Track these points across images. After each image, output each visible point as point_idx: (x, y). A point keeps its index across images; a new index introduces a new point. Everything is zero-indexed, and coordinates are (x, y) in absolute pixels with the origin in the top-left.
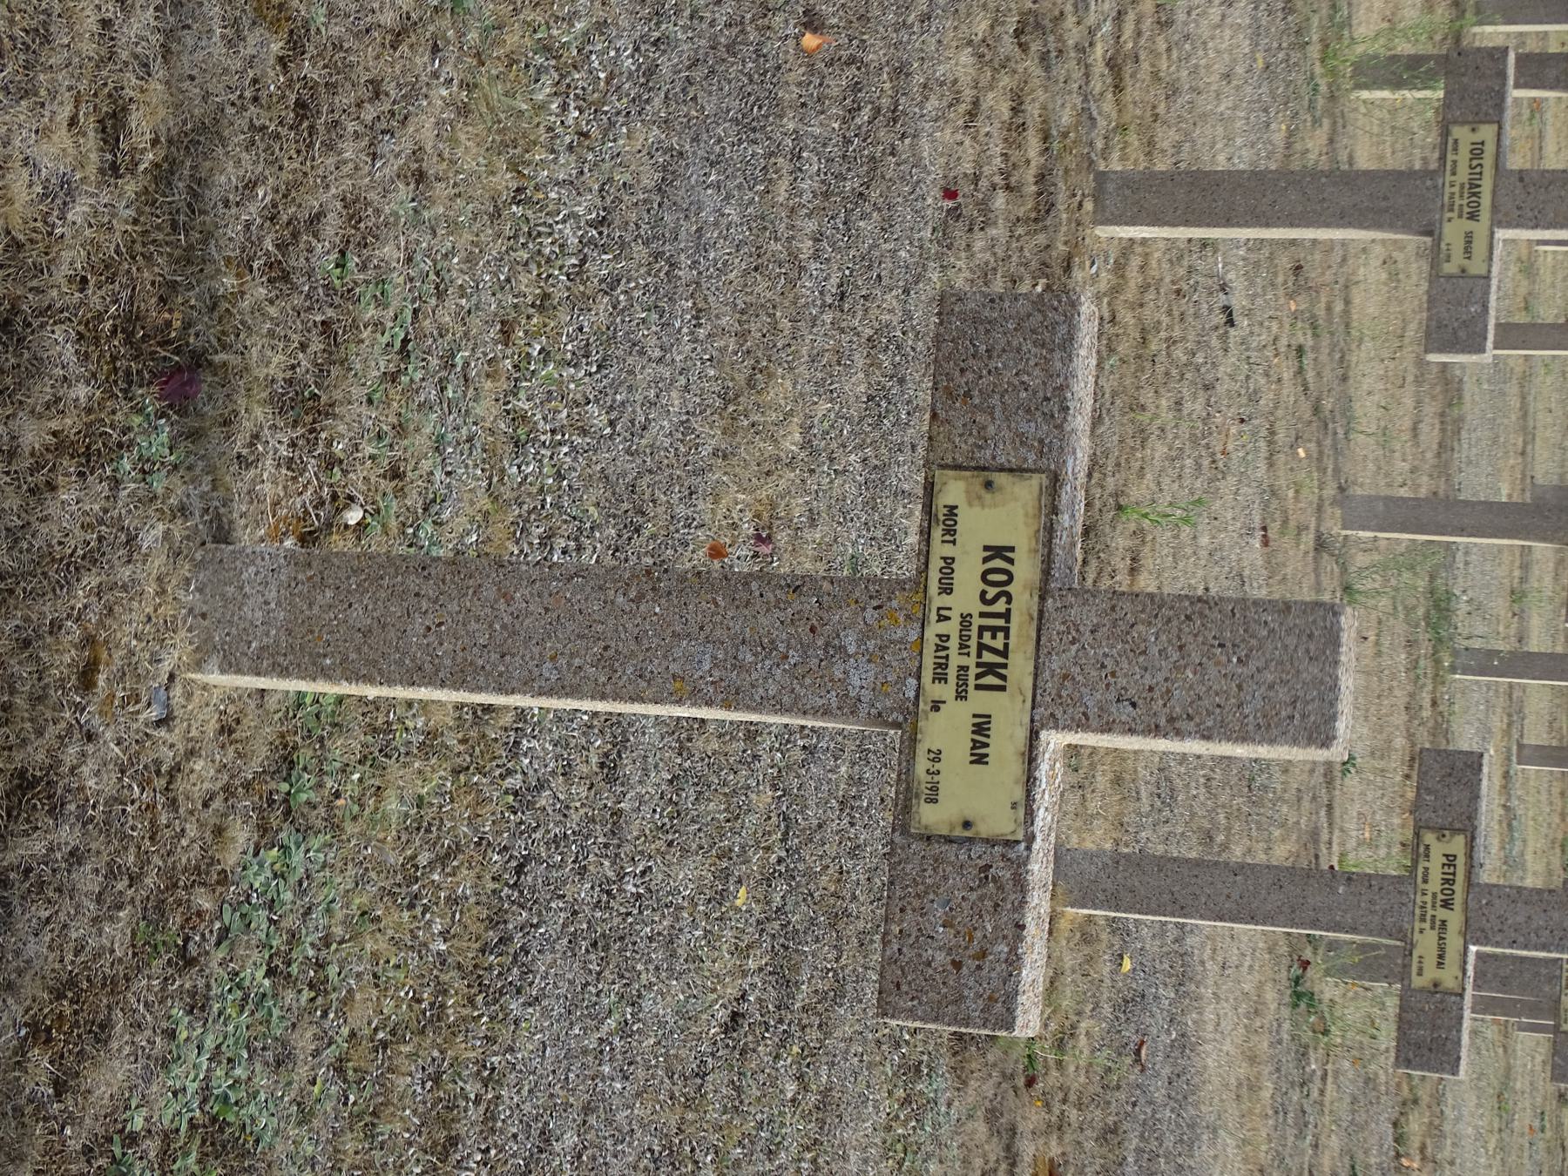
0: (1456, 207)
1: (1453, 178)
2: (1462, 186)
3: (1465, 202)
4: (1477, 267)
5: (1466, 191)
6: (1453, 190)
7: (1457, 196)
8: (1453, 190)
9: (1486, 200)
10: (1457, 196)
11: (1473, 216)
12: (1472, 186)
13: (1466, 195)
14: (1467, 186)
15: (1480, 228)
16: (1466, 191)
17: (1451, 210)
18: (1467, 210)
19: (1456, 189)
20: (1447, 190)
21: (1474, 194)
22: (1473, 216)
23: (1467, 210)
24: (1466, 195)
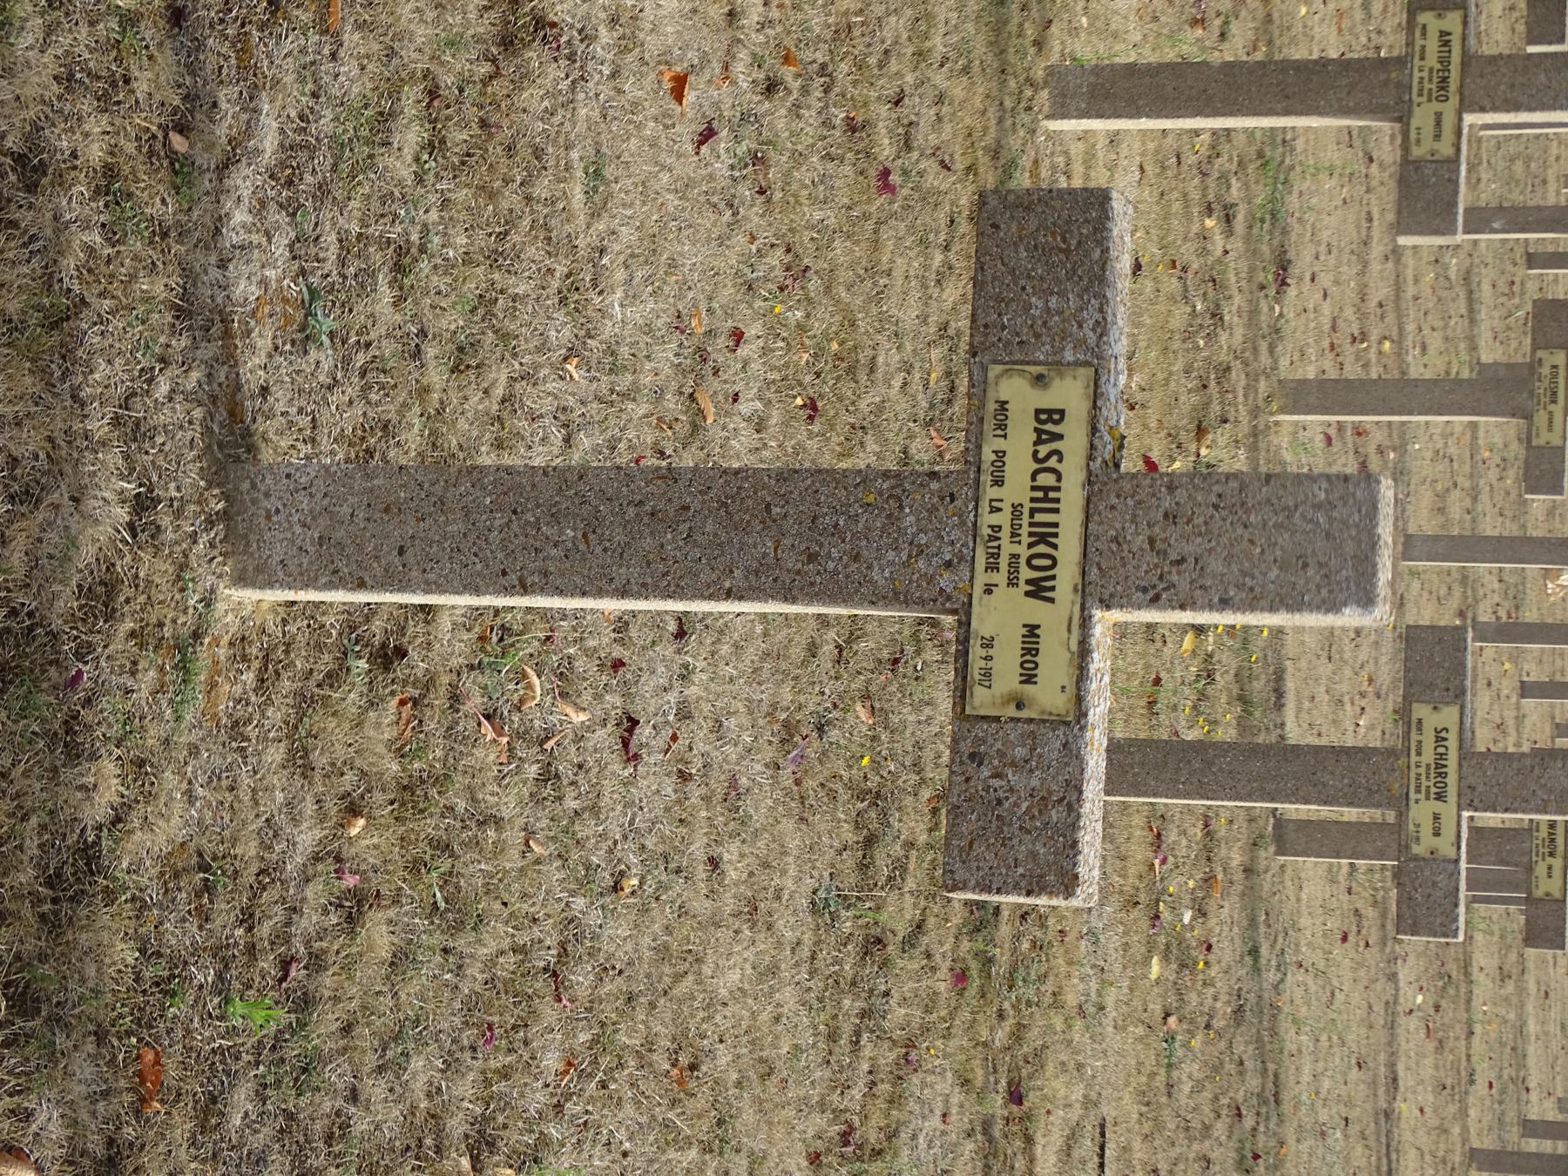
2: (1428, 766)
3: (1431, 784)
5: (1432, 771)
7: (1423, 777)
9: (1452, 779)
10: (1423, 777)
11: (1440, 797)
12: (1438, 766)
13: (1432, 775)
14: (1433, 766)
16: (1432, 771)
18: (1433, 790)
19: (1422, 770)
20: (1413, 771)
21: (1440, 774)
23: (1433, 790)
24: (1432, 775)
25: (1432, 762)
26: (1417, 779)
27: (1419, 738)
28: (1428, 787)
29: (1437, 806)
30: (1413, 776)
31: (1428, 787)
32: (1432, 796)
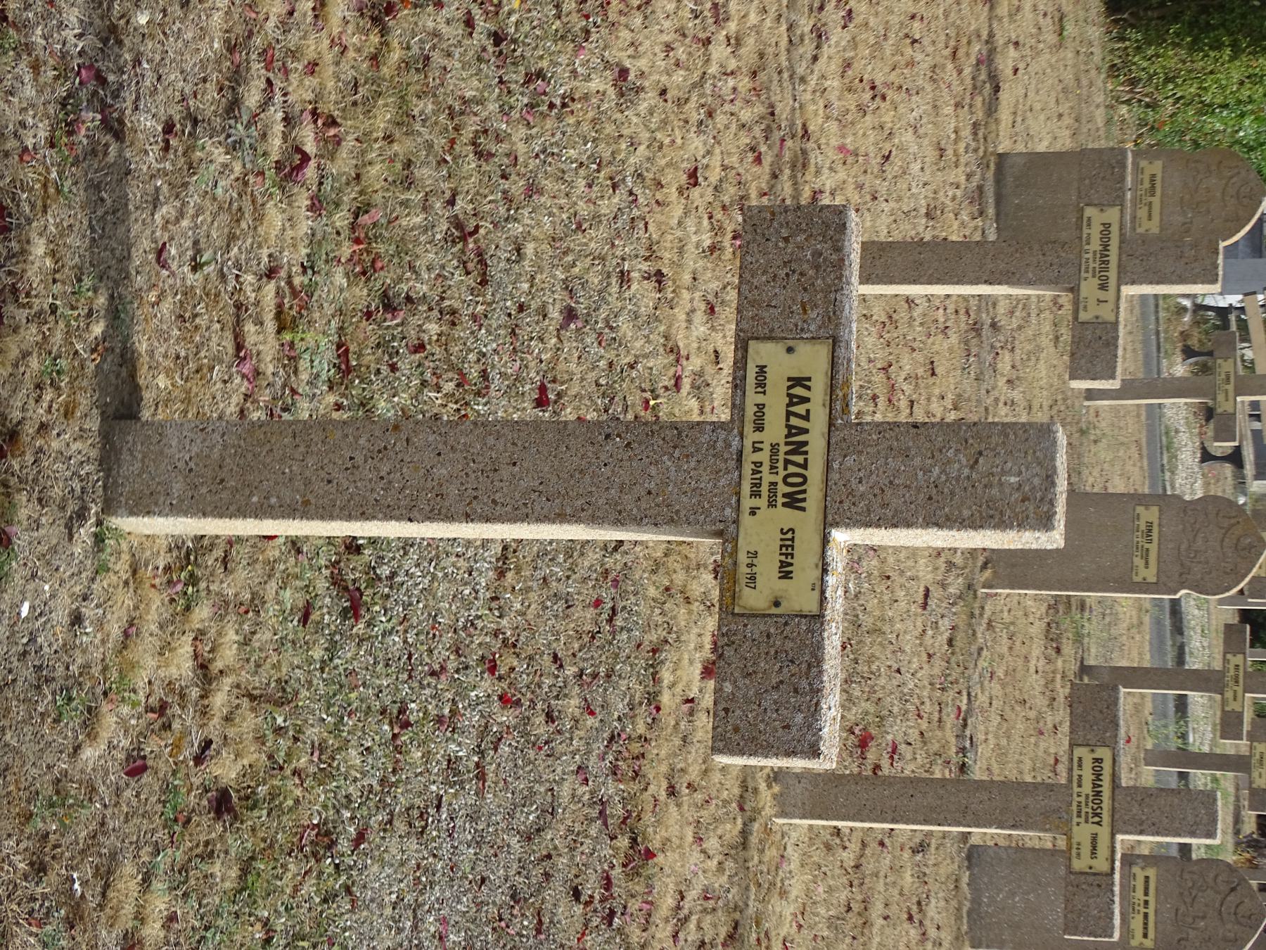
0: (765, 489)
1: (757, 436)
3: (779, 479)
4: (799, 598)
6: (757, 457)
7: (765, 468)
8: (757, 457)
10: (765, 468)
11: (794, 502)
15: (806, 523)
17: (756, 494)
18: (782, 489)
20: (750, 457)
22: (794, 502)
23: (782, 489)
24: (781, 465)
25: (781, 440)
26: (754, 472)
27: (760, 399)
28: (774, 484)
29: (787, 517)
30: (747, 469)
31: (774, 484)
32: (780, 500)
